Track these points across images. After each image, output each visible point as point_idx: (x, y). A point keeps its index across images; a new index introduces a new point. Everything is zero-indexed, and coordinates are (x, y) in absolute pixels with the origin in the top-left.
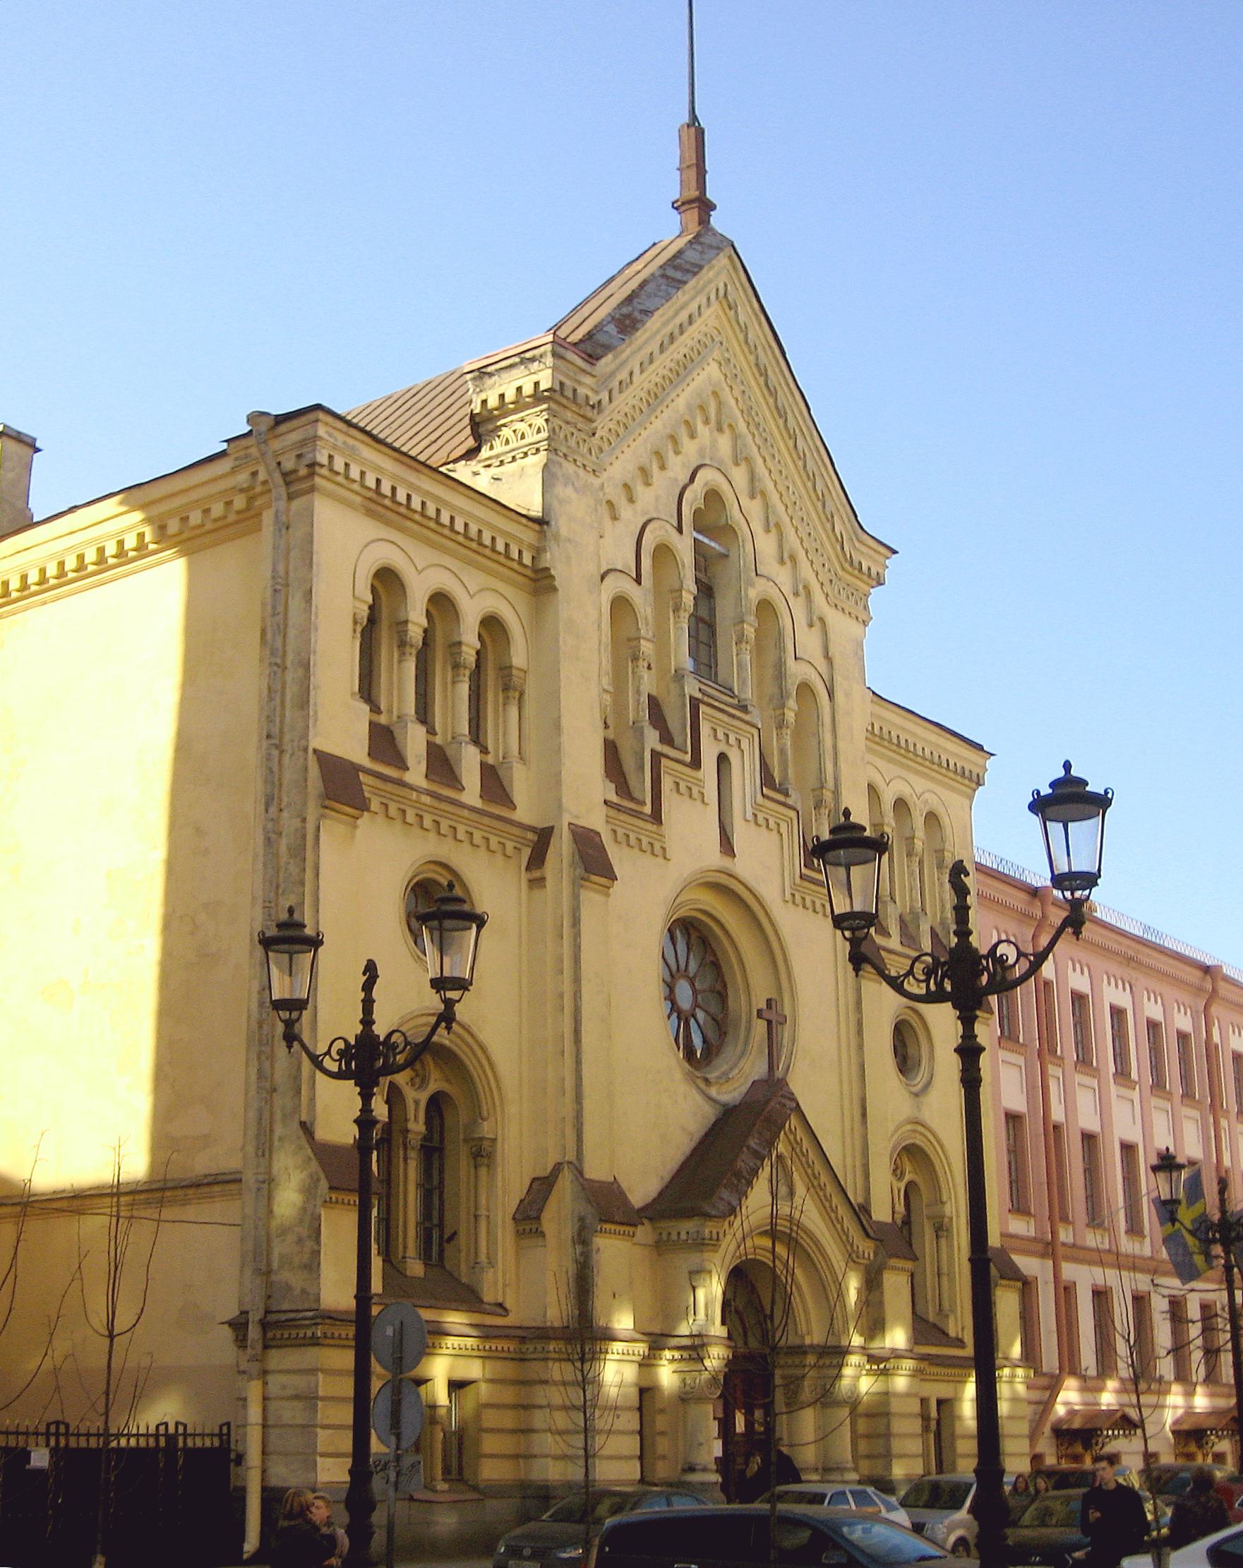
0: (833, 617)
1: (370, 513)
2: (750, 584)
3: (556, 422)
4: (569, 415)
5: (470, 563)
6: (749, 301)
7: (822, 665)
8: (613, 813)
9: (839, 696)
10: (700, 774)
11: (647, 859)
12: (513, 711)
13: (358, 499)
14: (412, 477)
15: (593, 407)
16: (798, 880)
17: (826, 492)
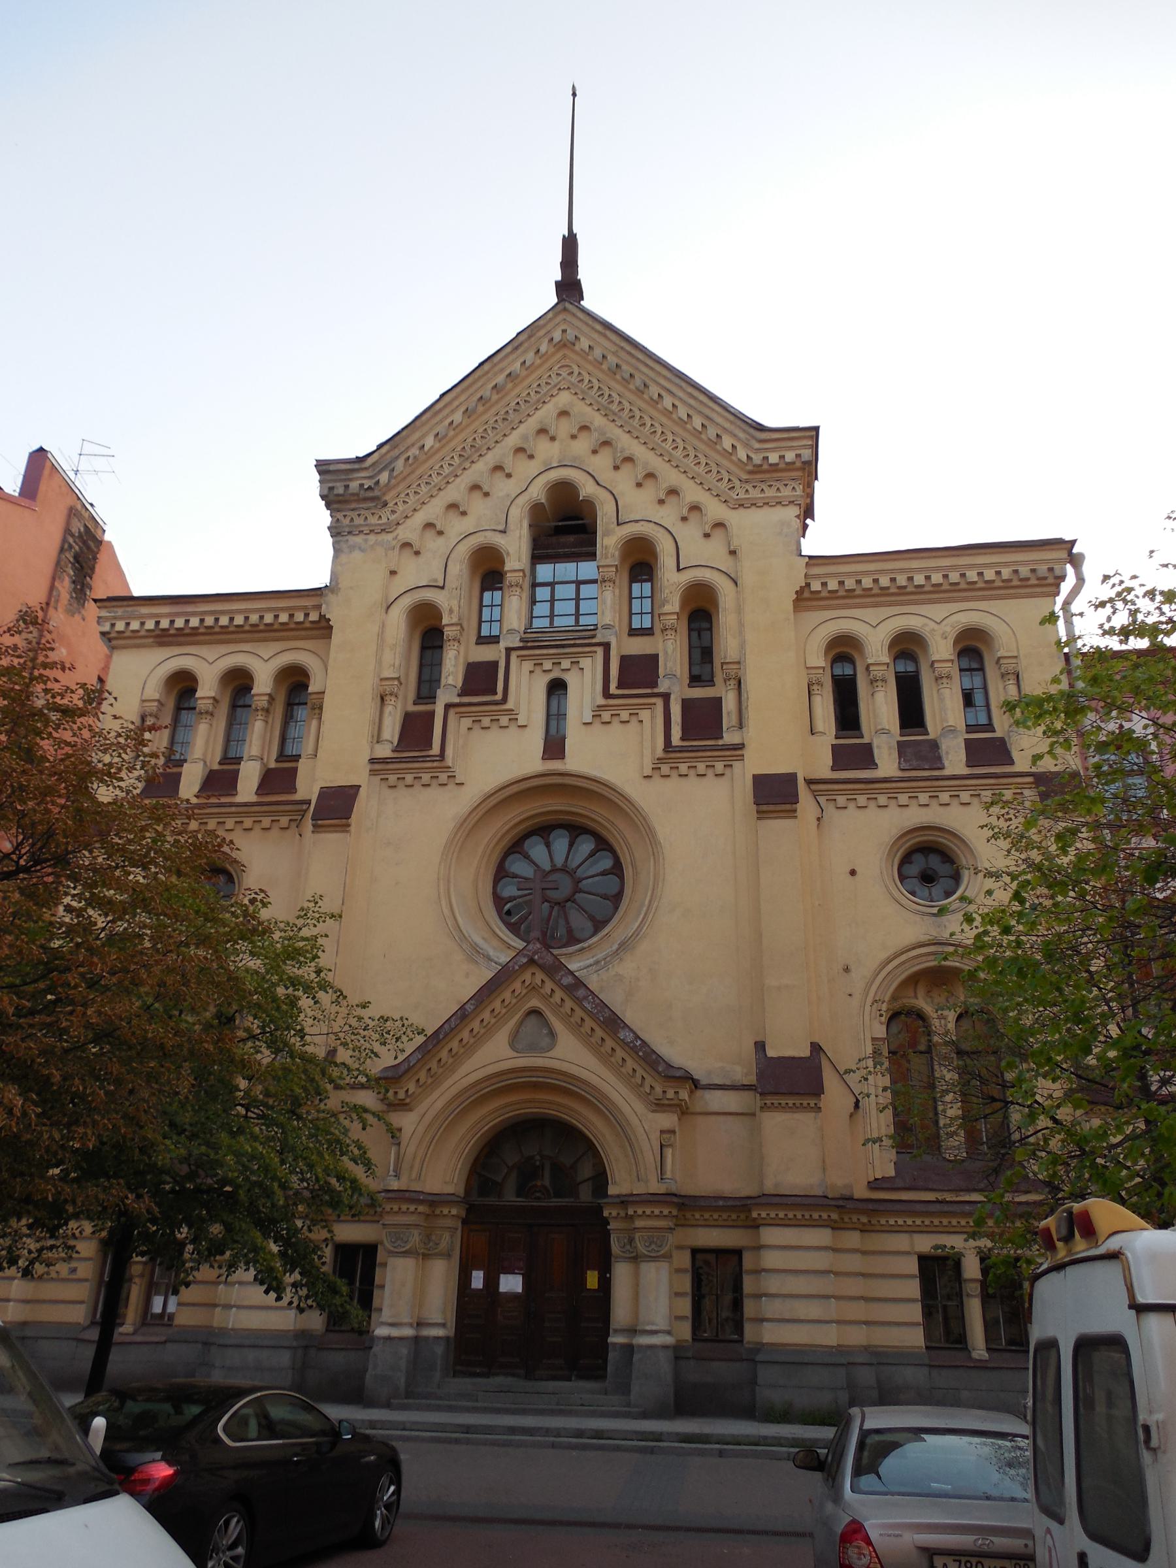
0: (734, 518)
1: (162, 644)
2: (607, 533)
3: (339, 515)
4: (353, 506)
5: (265, 640)
6: (593, 328)
7: (725, 563)
8: (377, 767)
9: (748, 578)
10: (510, 705)
11: (434, 792)
12: (314, 723)
13: (151, 640)
14: (190, 608)
15: (370, 488)
16: (659, 752)
17: (706, 423)
